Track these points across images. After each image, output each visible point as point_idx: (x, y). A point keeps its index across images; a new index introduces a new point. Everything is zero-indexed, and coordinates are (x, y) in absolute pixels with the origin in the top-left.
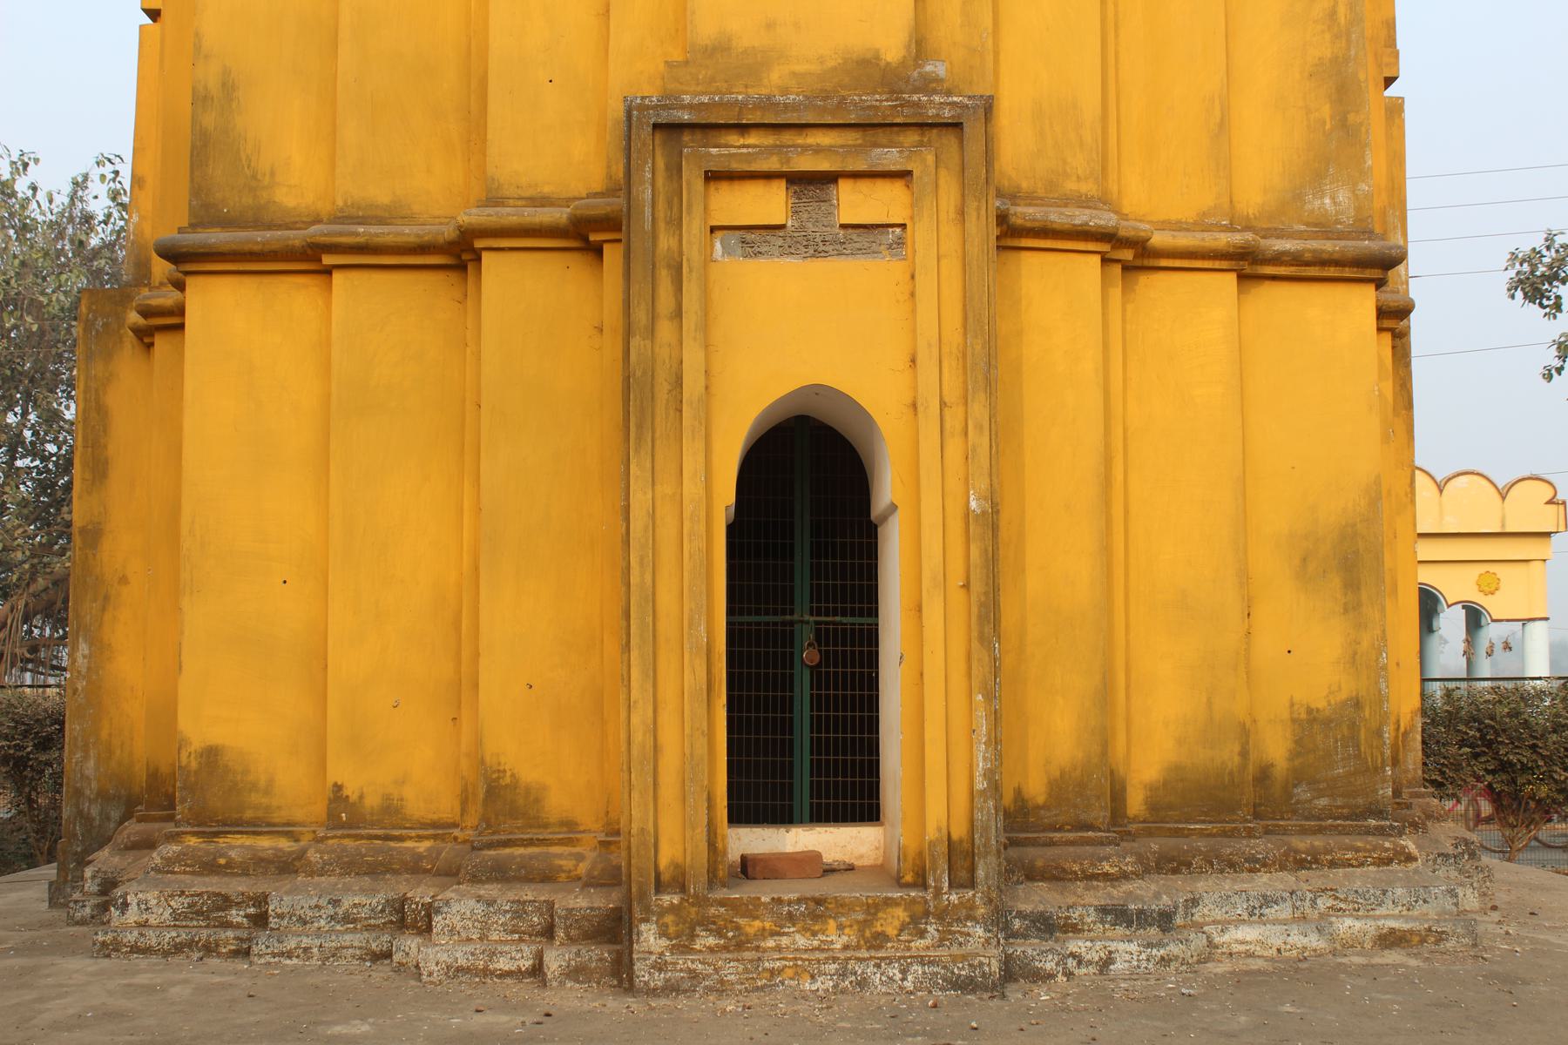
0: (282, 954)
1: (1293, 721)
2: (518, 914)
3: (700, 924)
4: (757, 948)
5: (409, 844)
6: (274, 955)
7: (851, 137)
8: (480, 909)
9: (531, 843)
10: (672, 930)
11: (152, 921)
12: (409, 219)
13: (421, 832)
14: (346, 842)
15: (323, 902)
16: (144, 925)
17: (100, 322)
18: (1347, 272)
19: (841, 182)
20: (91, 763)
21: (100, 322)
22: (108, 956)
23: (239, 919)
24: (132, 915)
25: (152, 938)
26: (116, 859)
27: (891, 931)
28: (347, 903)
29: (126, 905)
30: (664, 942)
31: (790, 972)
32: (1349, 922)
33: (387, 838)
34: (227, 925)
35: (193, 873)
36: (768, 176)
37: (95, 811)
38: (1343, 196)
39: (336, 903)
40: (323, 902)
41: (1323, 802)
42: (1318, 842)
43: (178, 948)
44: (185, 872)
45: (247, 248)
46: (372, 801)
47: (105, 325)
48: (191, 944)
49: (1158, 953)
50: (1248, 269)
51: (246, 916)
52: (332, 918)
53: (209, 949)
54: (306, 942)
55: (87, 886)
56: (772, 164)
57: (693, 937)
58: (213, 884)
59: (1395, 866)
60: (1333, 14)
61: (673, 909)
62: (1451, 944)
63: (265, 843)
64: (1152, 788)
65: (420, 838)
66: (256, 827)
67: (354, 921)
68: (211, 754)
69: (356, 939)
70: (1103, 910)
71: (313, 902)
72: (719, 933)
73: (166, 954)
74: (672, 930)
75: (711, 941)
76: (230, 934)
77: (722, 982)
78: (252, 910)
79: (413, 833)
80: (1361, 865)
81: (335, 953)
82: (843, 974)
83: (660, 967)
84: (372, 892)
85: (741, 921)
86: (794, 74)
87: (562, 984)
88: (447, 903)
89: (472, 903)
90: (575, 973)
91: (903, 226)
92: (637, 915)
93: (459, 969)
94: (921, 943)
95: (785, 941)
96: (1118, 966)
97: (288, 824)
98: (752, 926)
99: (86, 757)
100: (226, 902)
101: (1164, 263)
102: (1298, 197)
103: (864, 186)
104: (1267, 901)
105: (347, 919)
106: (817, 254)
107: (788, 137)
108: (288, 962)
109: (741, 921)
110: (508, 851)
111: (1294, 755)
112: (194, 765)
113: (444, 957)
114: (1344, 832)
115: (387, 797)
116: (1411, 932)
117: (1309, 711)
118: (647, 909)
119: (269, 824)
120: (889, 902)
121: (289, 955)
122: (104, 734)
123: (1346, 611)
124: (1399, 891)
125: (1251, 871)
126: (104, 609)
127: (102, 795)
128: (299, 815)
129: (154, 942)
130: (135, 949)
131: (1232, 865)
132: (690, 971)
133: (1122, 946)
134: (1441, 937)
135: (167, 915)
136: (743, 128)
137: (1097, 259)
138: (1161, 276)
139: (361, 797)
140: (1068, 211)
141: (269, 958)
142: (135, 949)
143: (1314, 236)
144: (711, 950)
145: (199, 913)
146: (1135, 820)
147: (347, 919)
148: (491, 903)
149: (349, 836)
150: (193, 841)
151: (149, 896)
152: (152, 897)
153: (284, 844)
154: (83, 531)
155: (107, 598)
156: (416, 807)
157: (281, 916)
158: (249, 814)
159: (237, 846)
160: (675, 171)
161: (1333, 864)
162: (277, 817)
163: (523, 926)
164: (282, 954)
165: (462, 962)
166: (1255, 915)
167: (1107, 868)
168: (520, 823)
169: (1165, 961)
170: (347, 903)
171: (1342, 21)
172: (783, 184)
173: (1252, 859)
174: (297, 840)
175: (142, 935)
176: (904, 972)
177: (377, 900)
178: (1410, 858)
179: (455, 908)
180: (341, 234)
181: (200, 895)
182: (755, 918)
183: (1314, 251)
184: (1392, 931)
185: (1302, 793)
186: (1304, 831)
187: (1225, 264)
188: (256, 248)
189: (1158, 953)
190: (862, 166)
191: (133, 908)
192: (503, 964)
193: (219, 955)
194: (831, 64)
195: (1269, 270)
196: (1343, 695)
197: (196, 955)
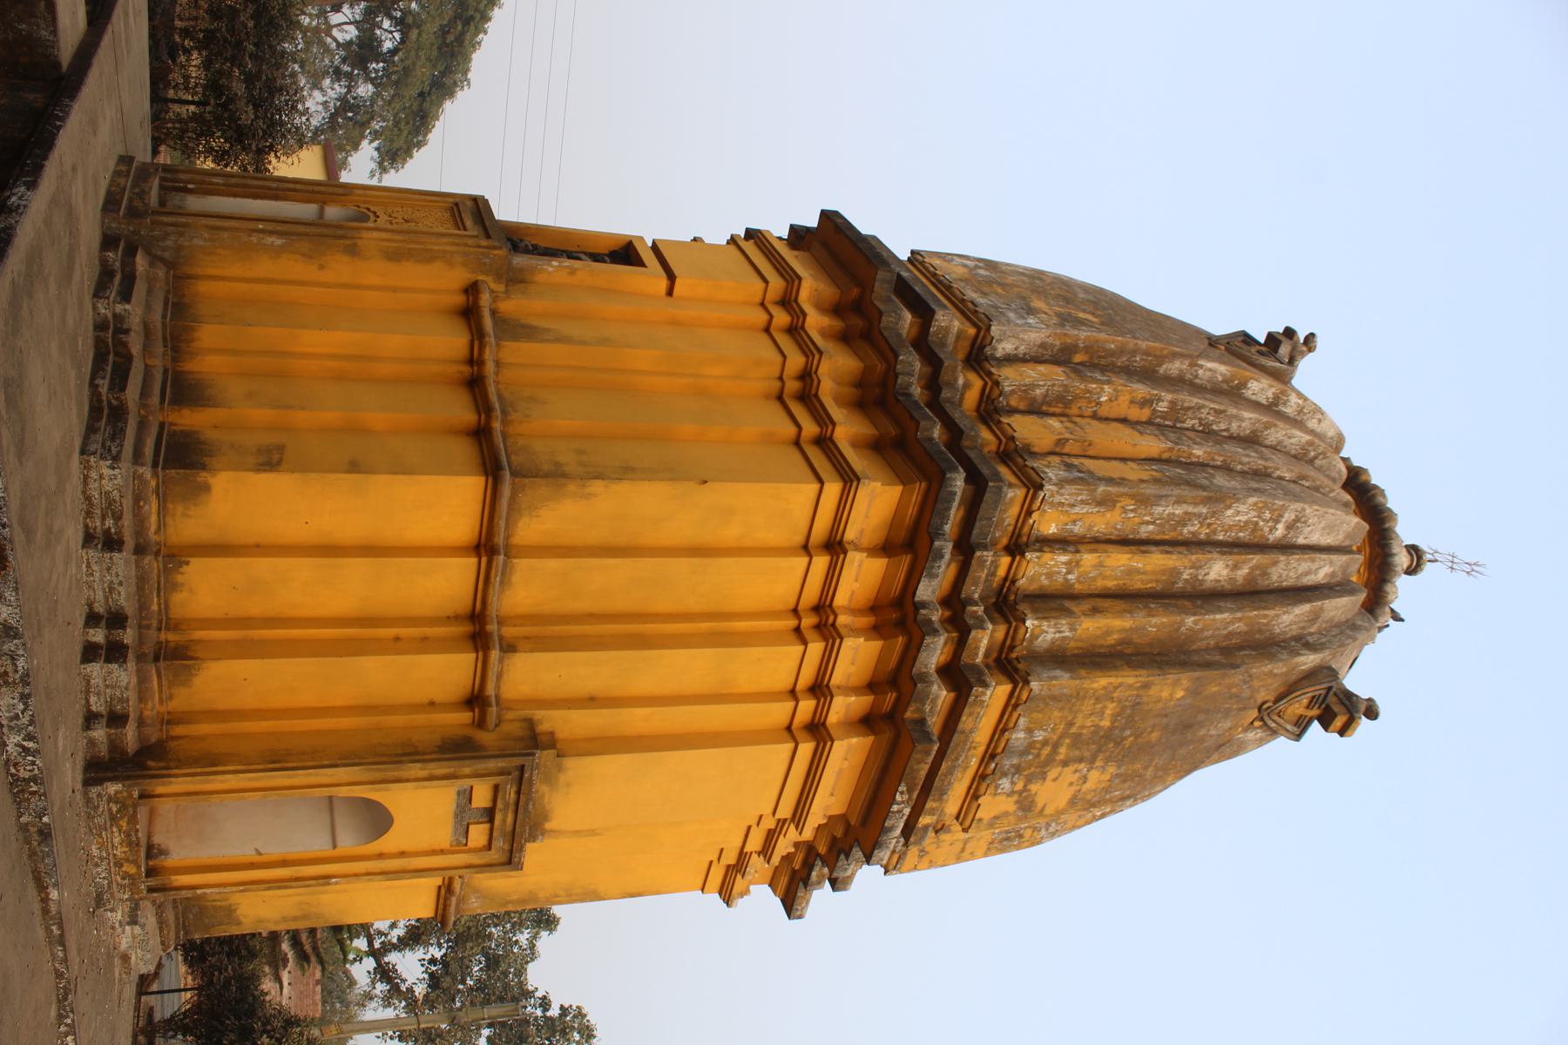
0: (88, 563)
2: (121, 700)
3: (123, 805)
4: (112, 825)
5: (156, 599)
6: (88, 560)
8: (123, 684)
9: (160, 685)
10: (119, 795)
11: (103, 482)
12: (502, 589)
13: (163, 607)
14: (156, 571)
15: (120, 578)
16: (101, 477)
17: (487, 260)
20: (201, 243)
21: (487, 260)
22: (81, 463)
23: (107, 524)
24: (106, 472)
25: (93, 485)
26: (137, 320)
27: (124, 869)
28: (120, 589)
29: (113, 468)
30: (112, 793)
31: (100, 840)
33: (159, 590)
34: (103, 518)
35: (134, 490)
36: (495, 801)
37: (169, 243)
38: (475, 905)
39: (121, 584)
40: (120, 578)
41: (191, 916)
43: (88, 499)
44: (134, 486)
45: (496, 516)
46: (180, 578)
47: (485, 264)
48: (91, 504)
49: (117, 925)
51: (109, 528)
52: (112, 582)
53: (89, 514)
54: (97, 575)
55: (119, 306)
56: (500, 805)
57: (116, 803)
58: (127, 503)
59: (160, 947)
61: (130, 796)
63: (154, 519)
65: (159, 604)
66: (162, 512)
67: (110, 592)
68: (206, 488)
69: (100, 596)
71: (120, 573)
72: (118, 812)
73: (84, 493)
74: (119, 795)
75: (114, 809)
76: (98, 524)
77: (93, 817)
78: (113, 530)
79: (162, 601)
81: (90, 587)
82: (102, 859)
83: (99, 795)
84: (127, 600)
85: (126, 819)
86: (544, 794)
87: (85, 738)
88: (126, 670)
89: (126, 681)
90: (92, 743)
91: (466, 845)
92: (126, 783)
93: (89, 681)
94: (119, 878)
95: (116, 834)
97: (165, 525)
98: (124, 823)
99: (205, 240)
100: (118, 517)
102: (476, 891)
103: (487, 832)
105: (111, 590)
106: (456, 815)
107: (512, 808)
108: (84, 566)
109: (126, 819)
110: (155, 678)
112: (199, 479)
113: (95, 674)
115: (182, 585)
116: (130, 964)
117: (235, 910)
118: (130, 786)
119: (164, 516)
120: (139, 867)
121: (88, 566)
122: (220, 251)
125: (157, 914)
126: (303, 255)
127: (180, 248)
128: (170, 530)
129: (91, 486)
130: (86, 478)
132: (98, 806)
135: (108, 488)
136: (518, 793)
139: (182, 573)
141: (85, 557)
142: (86, 478)
144: (110, 809)
145: (110, 504)
147: (111, 590)
148: (126, 689)
149: (159, 571)
150: (153, 483)
151: (119, 480)
152: (119, 481)
153: (153, 528)
154: (355, 245)
155: (310, 257)
156: (177, 598)
157: (111, 558)
158: (170, 506)
159: (152, 507)
160: (502, 773)
162: (169, 521)
163: (115, 702)
164: (88, 563)
165: (93, 682)
168: (171, 678)
170: (120, 589)
174: (155, 533)
175: (95, 480)
176: (104, 878)
177: (123, 602)
179: (123, 674)
180: (497, 571)
181: (121, 505)
182: (128, 823)
183: (450, 905)
188: (496, 521)
189: (117, 925)
190: (495, 834)
191: (111, 472)
192: (93, 699)
193: (85, 519)
194: (547, 806)
196: (243, 920)
197: (84, 506)
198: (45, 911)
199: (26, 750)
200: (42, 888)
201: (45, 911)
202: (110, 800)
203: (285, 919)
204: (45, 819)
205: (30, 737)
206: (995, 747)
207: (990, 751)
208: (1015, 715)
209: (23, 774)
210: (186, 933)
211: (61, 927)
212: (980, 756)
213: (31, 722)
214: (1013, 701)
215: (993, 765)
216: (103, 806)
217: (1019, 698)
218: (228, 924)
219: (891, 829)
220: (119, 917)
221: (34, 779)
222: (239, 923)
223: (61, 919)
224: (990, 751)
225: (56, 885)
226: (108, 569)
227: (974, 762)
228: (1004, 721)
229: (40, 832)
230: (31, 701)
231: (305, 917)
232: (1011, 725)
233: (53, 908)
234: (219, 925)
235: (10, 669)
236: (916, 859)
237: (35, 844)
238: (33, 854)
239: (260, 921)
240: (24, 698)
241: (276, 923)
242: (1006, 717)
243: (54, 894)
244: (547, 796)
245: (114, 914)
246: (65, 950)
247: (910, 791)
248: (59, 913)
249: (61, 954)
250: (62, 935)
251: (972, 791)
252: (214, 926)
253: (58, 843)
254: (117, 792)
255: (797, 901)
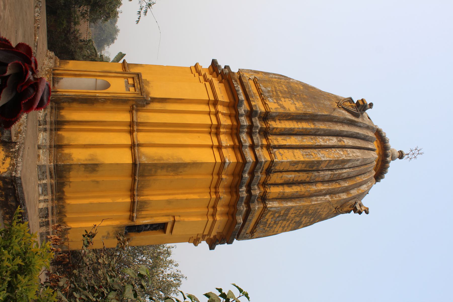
1: (70, 154)
7: (139, 88)
18: (134, 159)
19: (134, 88)
32: (42, 152)
41: (58, 156)
42: (53, 154)
49: (41, 117)
50: (132, 147)
57: (47, 71)
59: (49, 161)
60: (170, 159)
61: (51, 70)
62: (38, 162)
64: (61, 134)
70: (47, 114)
72: (48, 73)
75: (47, 73)
80: (49, 158)
96: (39, 113)
98: (48, 76)
101: (132, 136)
102: (144, 155)
103: (134, 89)
104: (46, 140)
111: (65, 153)
114: (54, 157)
123: (86, 159)
124: (46, 158)
125: (50, 142)
131: (51, 140)
133: (42, 114)
134: (39, 161)
136: (139, 80)
137: (130, 121)
138: (130, 137)
140: (135, 116)
143: (138, 157)
144: (46, 73)
146: (57, 133)
158: (61, 65)
161: (50, 155)
166: (44, 139)
167: (52, 117)
169: (40, 118)
171: (169, 160)
172: (133, 83)
173: (51, 142)
178: (50, 163)
182: (49, 76)
184: (40, 156)
185: (60, 154)
186: (54, 153)
187: (132, 142)
189: (41, 117)
195: (133, 150)
196: (74, 159)
198: (35, 40)
199: (38, 16)
200: (35, 36)
201: (35, 40)
202: (46, 70)
203: (86, 160)
204: (39, 26)
205: (40, 14)
206: (260, 92)
207: (260, 94)
208: (258, 84)
209: (37, 19)
210: (57, 162)
211: (37, 44)
212: (259, 96)
213: (40, 12)
214: (255, 82)
215: (263, 95)
216: (44, 70)
217: (256, 81)
218: (69, 160)
219: (238, 91)
220: (42, 115)
221: (38, 20)
222: (73, 160)
223: (38, 42)
224: (260, 94)
225: (38, 36)
226: (49, 61)
227: (258, 97)
228: (257, 87)
229: (38, 27)
230: (41, 10)
231: (92, 160)
232: (259, 86)
233: (36, 40)
234: (66, 160)
235: (39, 6)
236: (280, 156)
237: (36, 29)
238: (35, 30)
239: (79, 160)
240: (40, 9)
241: (84, 161)
242: (257, 86)
243: (37, 38)
244: (148, 89)
245: (40, 113)
246: (37, 48)
247: (236, 81)
248: (37, 41)
249: (36, 49)
250: (37, 45)
251: (264, 104)
252: (65, 160)
253: (40, 30)
254: (48, 69)
255: (245, 156)
